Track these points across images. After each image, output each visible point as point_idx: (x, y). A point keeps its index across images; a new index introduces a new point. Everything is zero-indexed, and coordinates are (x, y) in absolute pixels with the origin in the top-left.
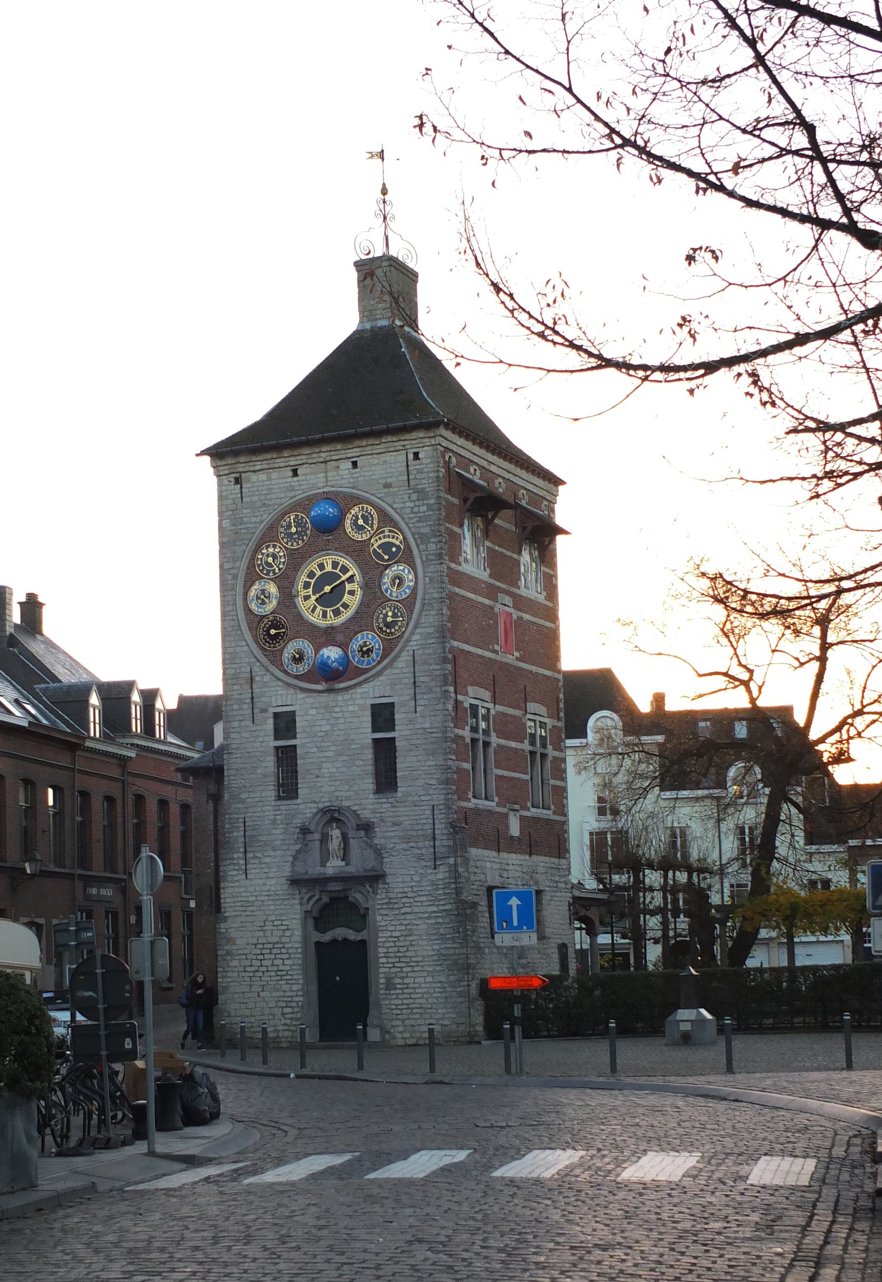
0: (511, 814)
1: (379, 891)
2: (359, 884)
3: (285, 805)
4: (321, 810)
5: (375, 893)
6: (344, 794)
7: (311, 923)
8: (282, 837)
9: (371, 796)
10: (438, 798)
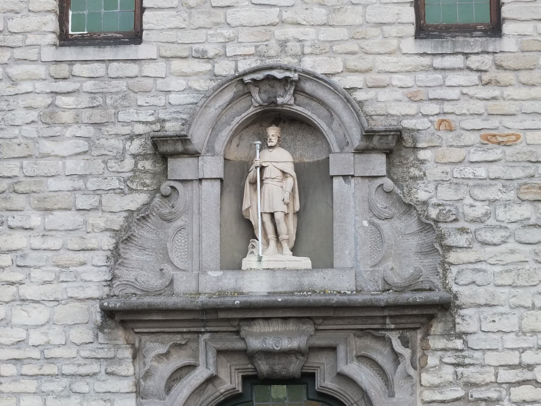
1: (432, 360)
2: (363, 333)
3: (89, 63)
4: (239, 79)
5: (419, 365)
6: (310, 34)
8: (75, 166)
9: (410, 45)
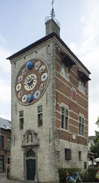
0: (73, 134)
4: (27, 131)
5: (37, 149)
7: (25, 155)
8: (20, 138)
10: (51, 126)
